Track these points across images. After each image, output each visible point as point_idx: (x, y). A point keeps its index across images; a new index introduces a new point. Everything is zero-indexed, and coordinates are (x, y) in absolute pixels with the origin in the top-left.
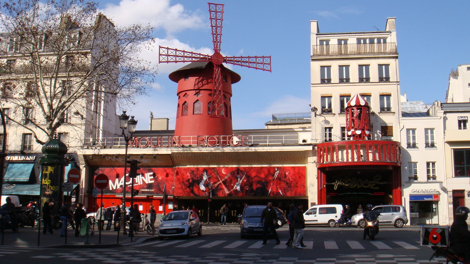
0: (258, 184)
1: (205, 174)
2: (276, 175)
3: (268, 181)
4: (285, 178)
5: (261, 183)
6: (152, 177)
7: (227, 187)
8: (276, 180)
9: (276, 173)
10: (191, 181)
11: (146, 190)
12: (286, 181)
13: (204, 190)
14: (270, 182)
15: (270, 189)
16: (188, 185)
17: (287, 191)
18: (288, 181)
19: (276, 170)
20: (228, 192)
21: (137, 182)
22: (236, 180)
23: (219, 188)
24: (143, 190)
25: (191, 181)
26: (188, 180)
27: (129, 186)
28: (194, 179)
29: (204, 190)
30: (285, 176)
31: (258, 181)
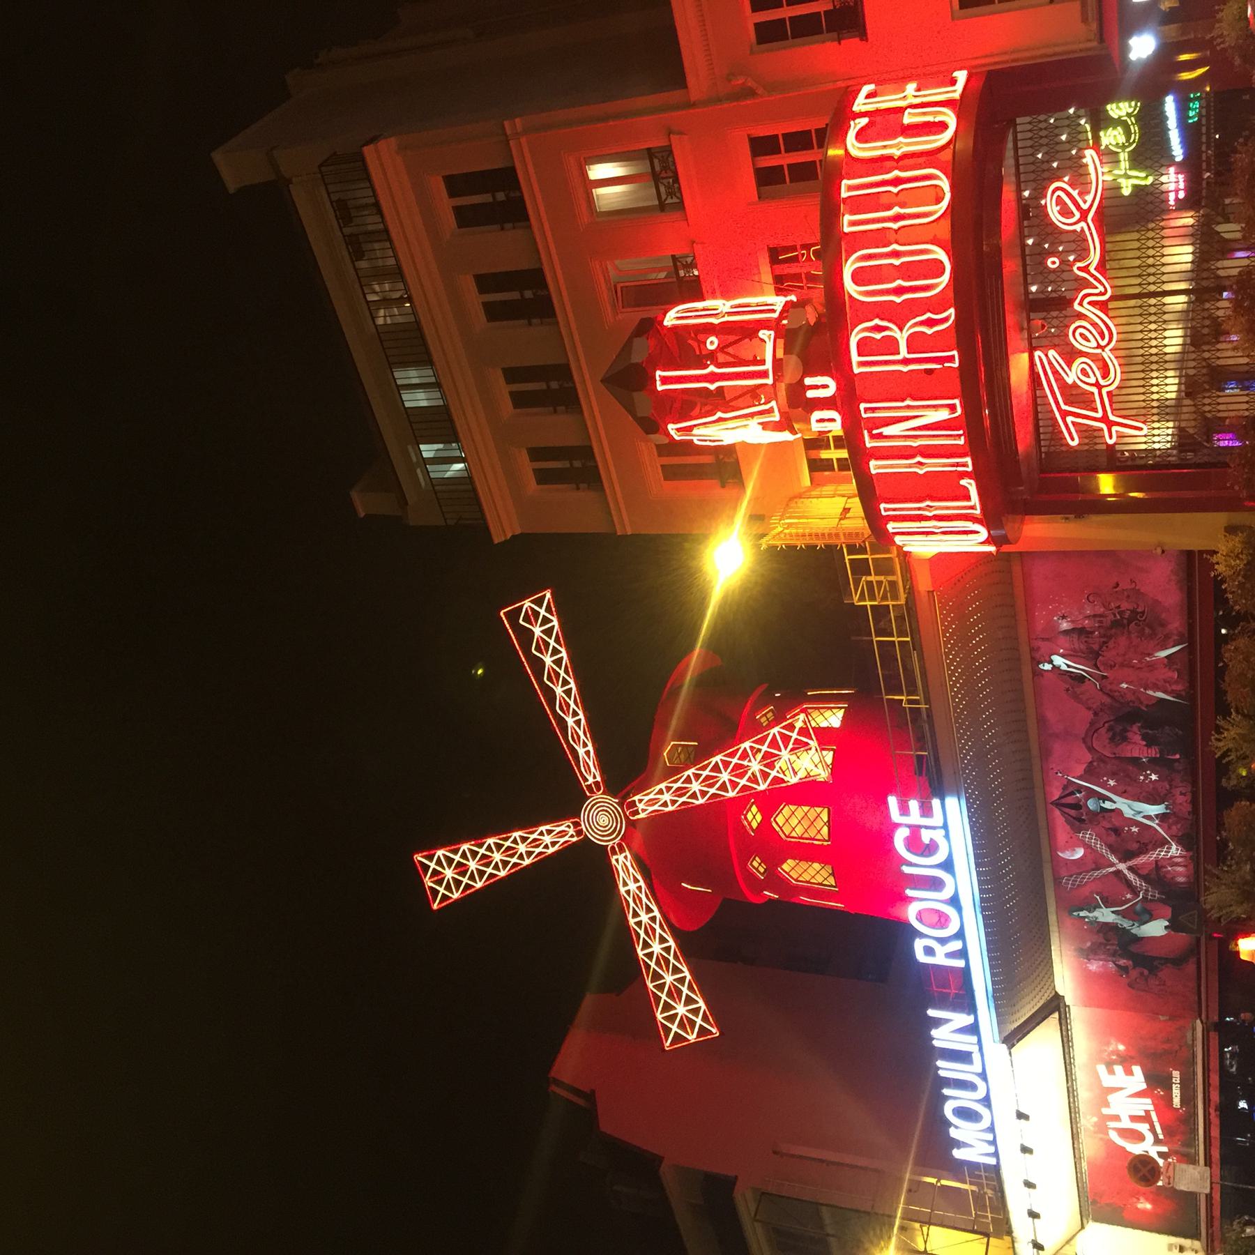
0: (1125, 739)
1: (1091, 915)
2: (1079, 668)
3: (1108, 700)
4: (1093, 633)
5: (1121, 728)
6: (1118, 1069)
7: (1143, 849)
8: (1101, 668)
9: (1064, 667)
10: (1122, 962)
11: (1176, 1092)
12: (1102, 631)
13: (1167, 923)
14: (1110, 690)
15: (1150, 692)
16: (1146, 972)
17: (1163, 625)
18: (1107, 622)
19: (1047, 667)
20: (1174, 847)
21: (1143, 1114)
22: (1112, 814)
23: (1153, 876)
24: (1177, 1101)
25: (1122, 962)
26: (1124, 969)
27: (1161, 1137)
28: (1115, 952)
29: (1167, 923)
30: (1080, 632)
31: (1112, 739)
